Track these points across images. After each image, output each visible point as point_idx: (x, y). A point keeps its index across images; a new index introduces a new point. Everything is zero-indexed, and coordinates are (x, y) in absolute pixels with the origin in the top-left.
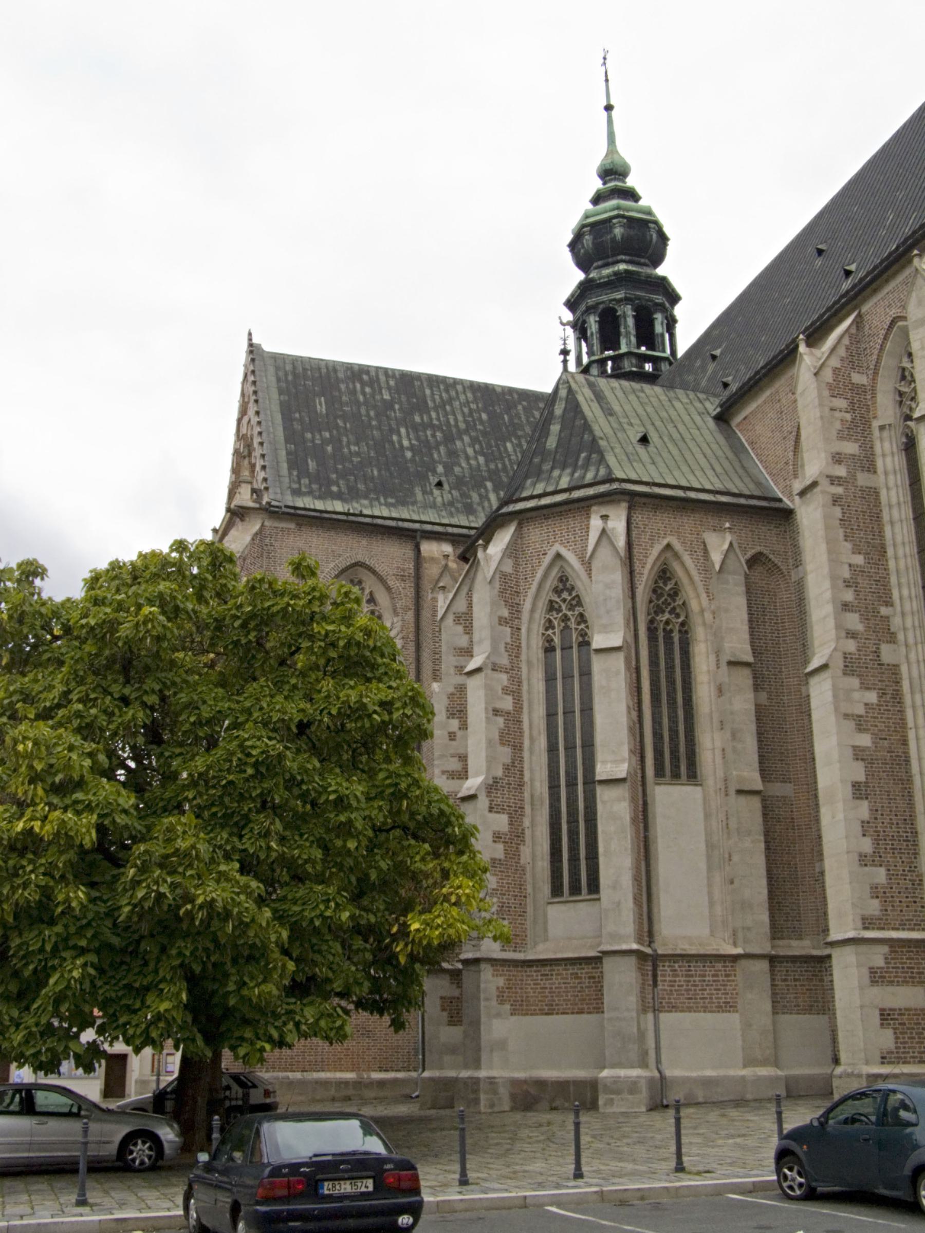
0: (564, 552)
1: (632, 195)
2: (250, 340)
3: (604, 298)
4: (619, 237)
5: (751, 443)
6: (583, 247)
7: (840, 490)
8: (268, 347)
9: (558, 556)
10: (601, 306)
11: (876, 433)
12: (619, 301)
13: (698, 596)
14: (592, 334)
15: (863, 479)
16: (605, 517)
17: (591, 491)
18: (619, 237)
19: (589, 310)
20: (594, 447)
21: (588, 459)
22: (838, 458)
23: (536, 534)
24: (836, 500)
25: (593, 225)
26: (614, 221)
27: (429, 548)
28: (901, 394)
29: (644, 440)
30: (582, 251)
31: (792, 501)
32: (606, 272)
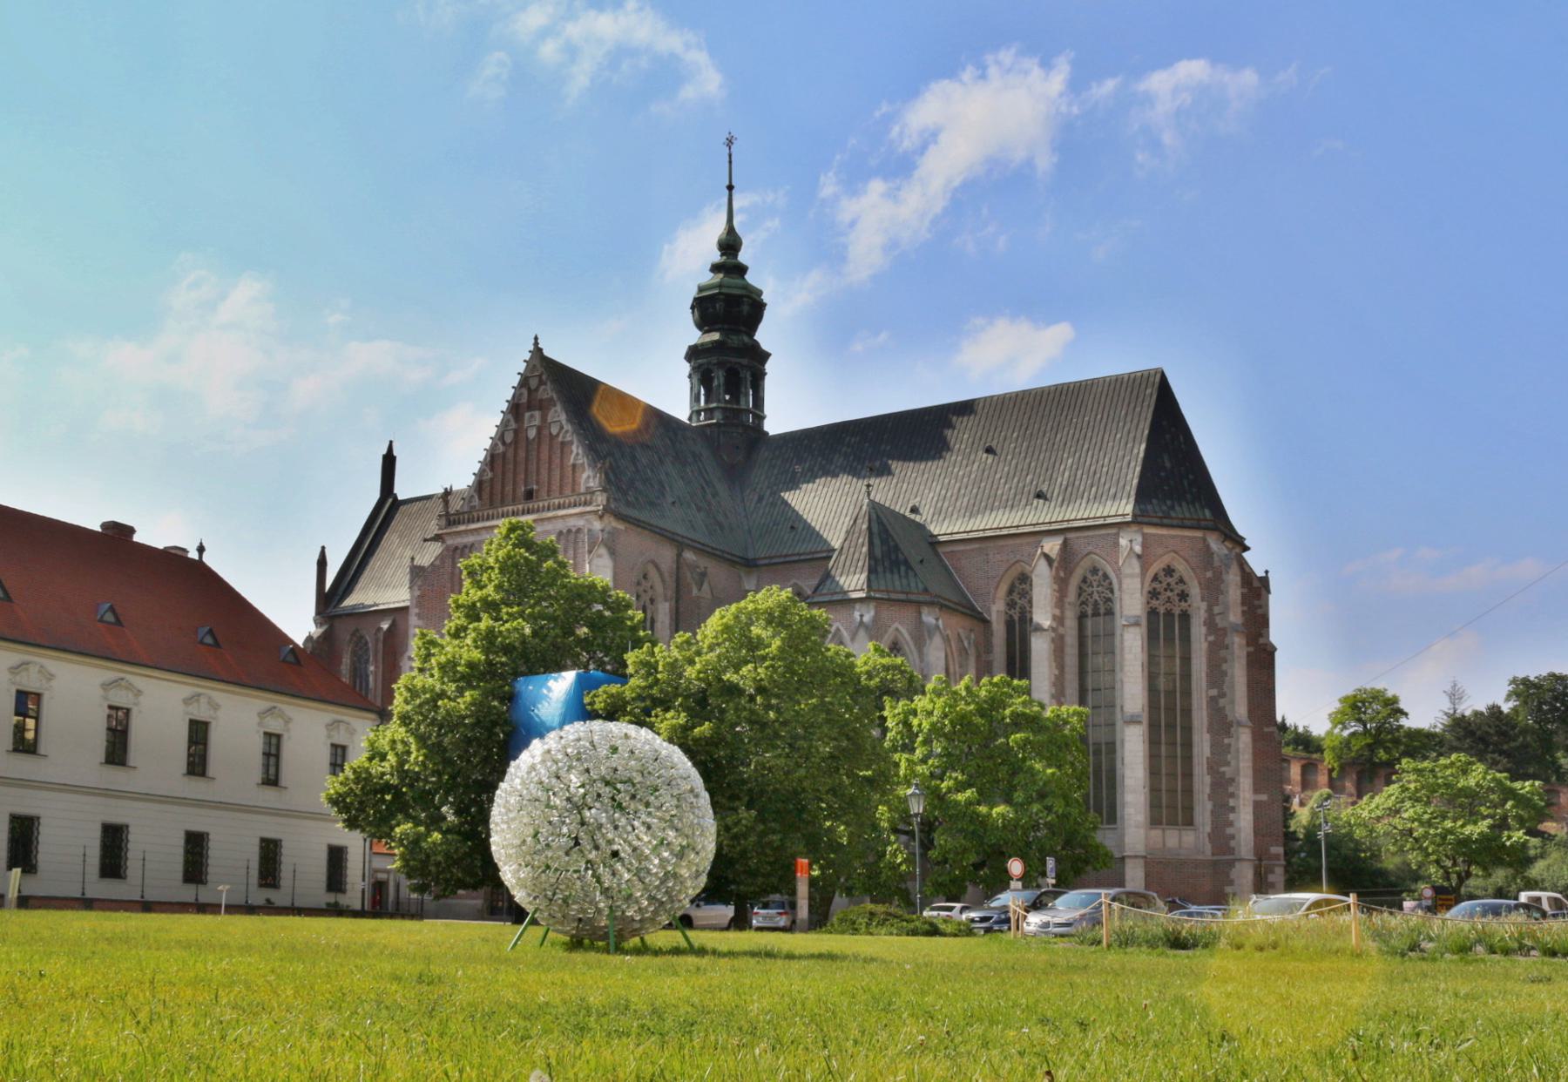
0: (900, 628)
1: (741, 270)
2: (536, 343)
3: (733, 360)
4: (745, 312)
5: (955, 568)
6: (714, 307)
7: (1053, 635)
8: (546, 353)
9: (897, 629)
10: (728, 365)
11: (1067, 606)
12: (742, 366)
13: (954, 665)
14: (719, 385)
15: (1061, 630)
16: (937, 619)
17: (921, 598)
18: (745, 312)
19: (720, 365)
20: (906, 563)
21: (907, 573)
22: (1055, 618)
23: (886, 613)
24: (1053, 640)
25: (727, 295)
26: (745, 299)
27: (689, 555)
28: (1080, 588)
29: (922, 561)
30: (711, 310)
31: (990, 615)
32: (734, 337)
